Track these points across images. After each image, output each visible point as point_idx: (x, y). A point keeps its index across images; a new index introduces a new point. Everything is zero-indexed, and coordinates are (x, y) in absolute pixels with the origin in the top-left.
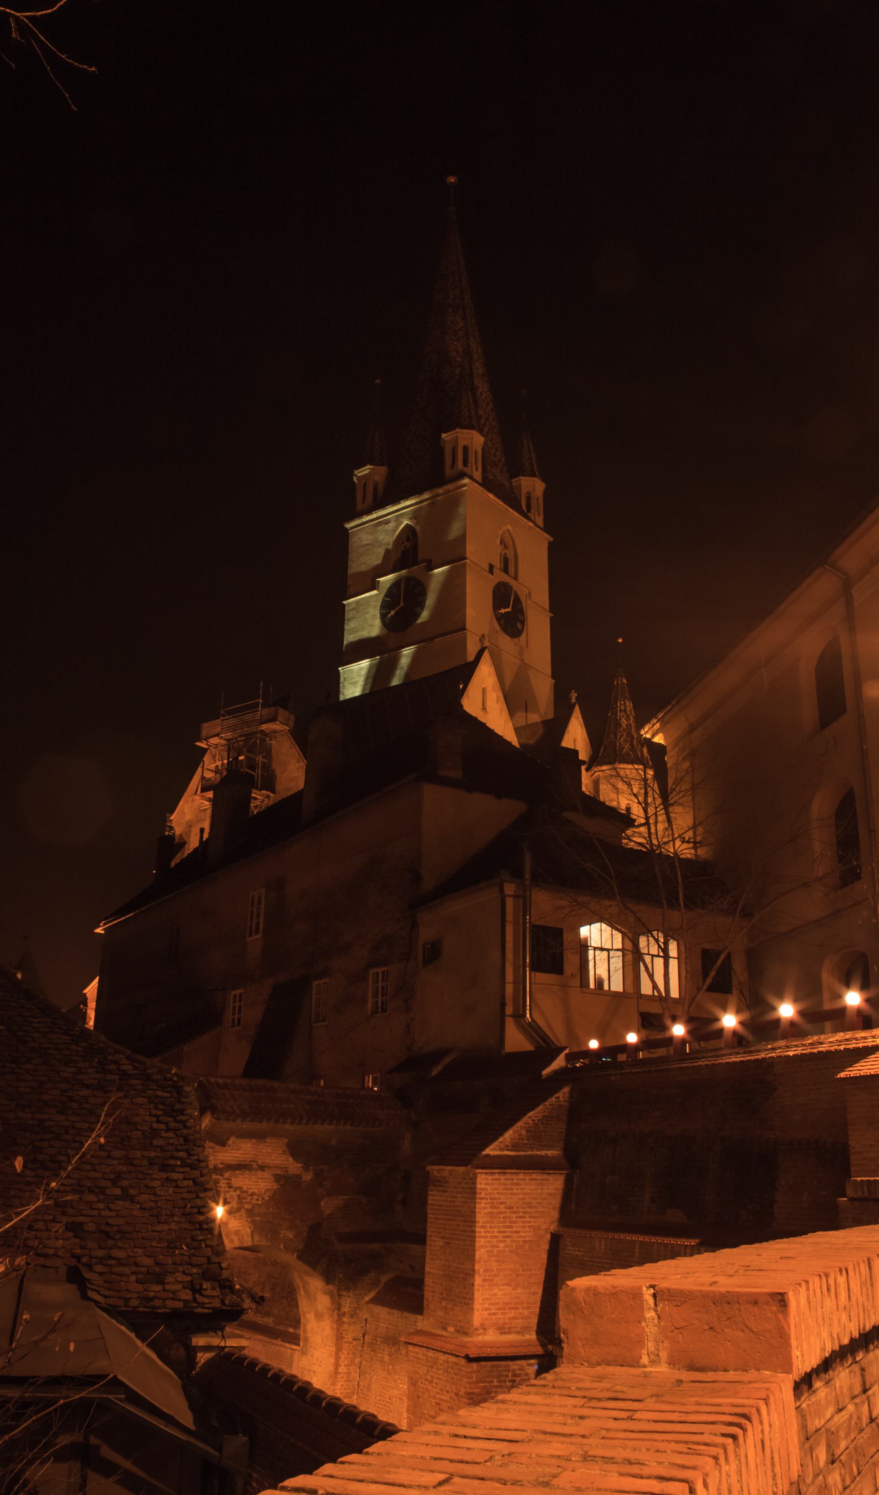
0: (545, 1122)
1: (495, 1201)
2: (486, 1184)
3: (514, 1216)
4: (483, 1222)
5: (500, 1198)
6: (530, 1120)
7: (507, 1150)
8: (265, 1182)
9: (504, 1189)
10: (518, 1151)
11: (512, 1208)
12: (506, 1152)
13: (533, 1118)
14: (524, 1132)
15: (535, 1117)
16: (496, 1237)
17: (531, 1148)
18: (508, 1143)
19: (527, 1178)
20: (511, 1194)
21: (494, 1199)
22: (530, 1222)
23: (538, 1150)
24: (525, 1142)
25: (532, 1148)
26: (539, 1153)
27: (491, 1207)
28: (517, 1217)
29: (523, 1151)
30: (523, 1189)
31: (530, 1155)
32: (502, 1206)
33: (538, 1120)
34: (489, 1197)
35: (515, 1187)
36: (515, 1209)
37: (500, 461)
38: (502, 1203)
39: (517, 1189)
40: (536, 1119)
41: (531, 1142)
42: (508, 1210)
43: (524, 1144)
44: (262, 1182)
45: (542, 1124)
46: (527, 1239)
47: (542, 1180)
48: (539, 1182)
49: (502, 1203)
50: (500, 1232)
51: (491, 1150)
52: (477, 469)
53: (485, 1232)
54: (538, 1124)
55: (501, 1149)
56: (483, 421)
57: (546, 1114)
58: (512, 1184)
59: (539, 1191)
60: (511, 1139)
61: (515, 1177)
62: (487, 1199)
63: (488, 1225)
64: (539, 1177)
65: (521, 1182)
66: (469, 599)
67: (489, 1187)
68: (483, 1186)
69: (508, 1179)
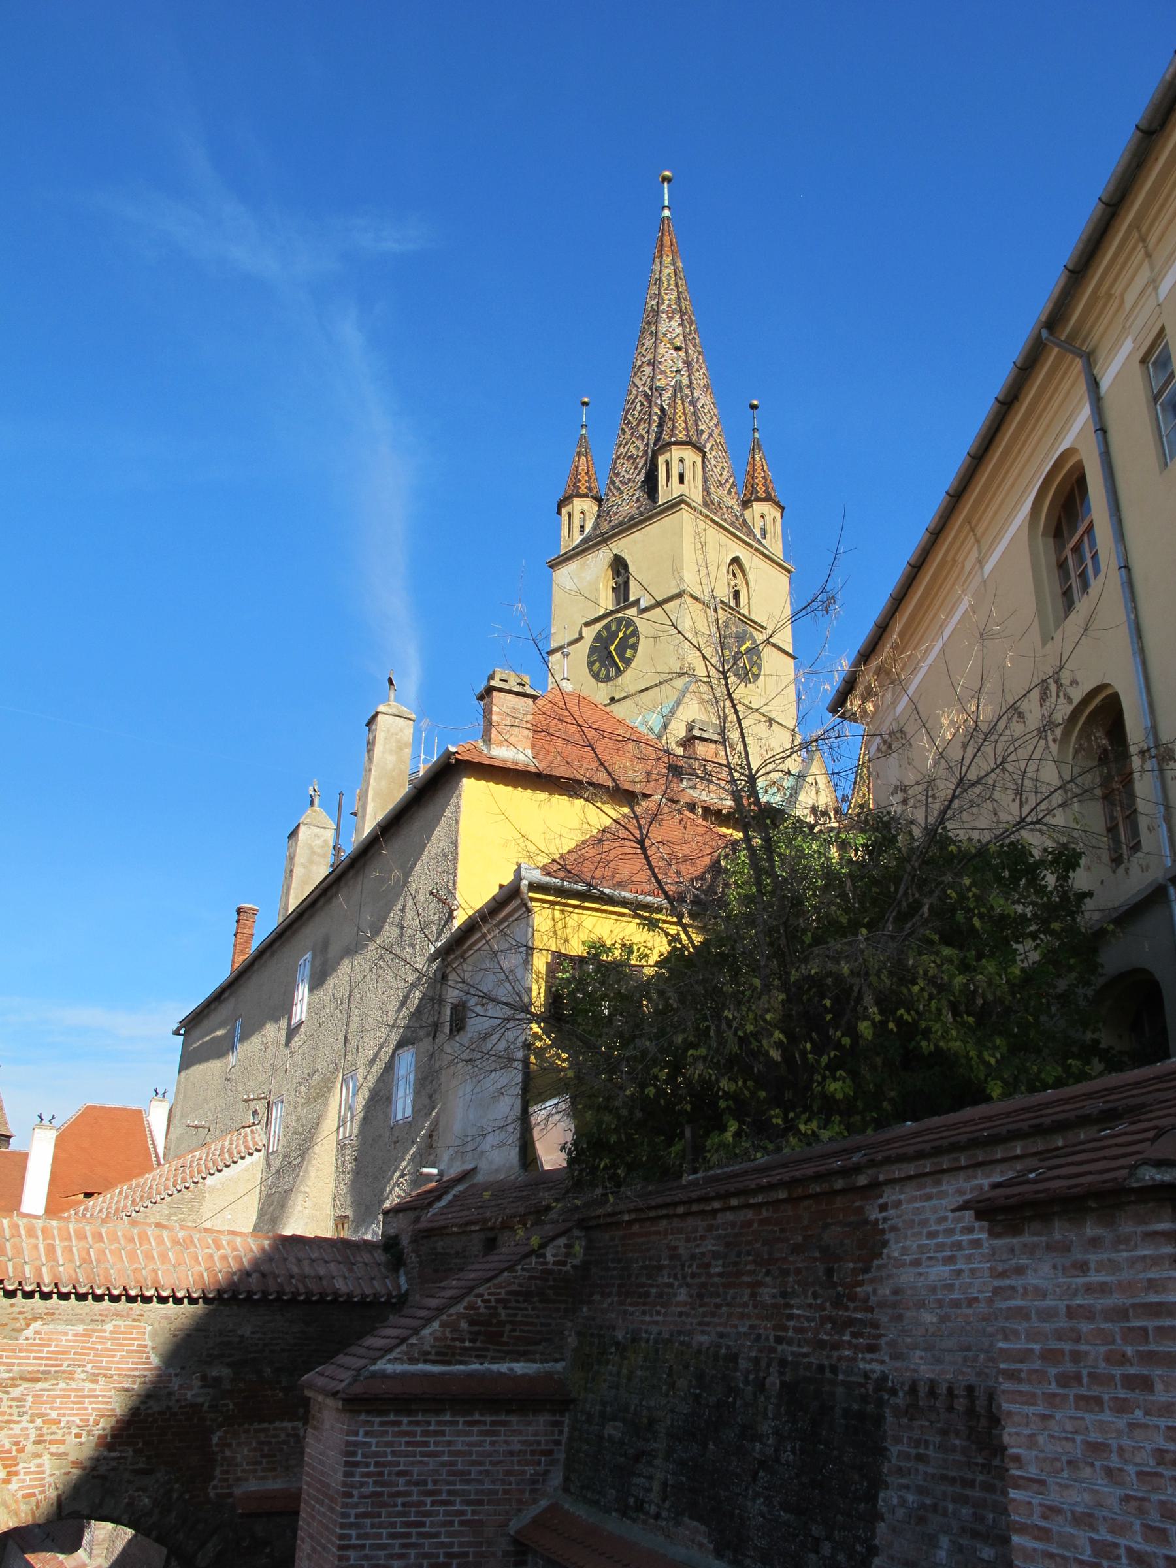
0: (513, 1304)
1: (386, 1470)
2: (367, 1434)
3: (429, 1500)
4: (357, 1516)
5: (398, 1464)
6: (479, 1300)
7: (426, 1361)
8: (96, 1403)
9: (408, 1443)
10: (449, 1363)
11: (425, 1483)
12: (421, 1367)
13: (486, 1297)
14: (464, 1325)
15: (489, 1294)
16: (383, 1547)
17: (477, 1357)
18: (427, 1348)
19: (461, 1420)
20: (423, 1454)
21: (384, 1465)
22: (463, 1513)
23: (494, 1360)
24: (467, 1344)
25: (481, 1358)
26: (494, 1367)
27: (376, 1483)
28: (433, 1503)
29: (461, 1363)
30: (449, 1443)
31: (470, 1375)
32: (401, 1480)
33: (498, 1301)
34: (372, 1461)
35: (432, 1440)
36: (430, 1487)
37: (727, 481)
38: (400, 1474)
39: (436, 1444)
40: (492, 1298)
41: (478, 1344)
42: (415, 1489)
43: (466, 1349)
44: (91, 1403)
45: (505, 1308)
46: (456, 1549)
47: (493, 1423)
48: (488, 1428)
49: (400, 1474)
50: (392, 1536)
51: (389, 1361)
52: (696, 487)
53: (359, 1537)
54: (496, 1308)
55: (412, 1360)
56: (705, 436)
57: (515, 1288)
58: (426, 1433)
59: (488, 1447)
60: (436, 1339)
61: (433, 1419)
62: (367, 1465)
63: (368, 1521)
64: (488, 1419)
65: (447, 1429)
67: (374, 1440)
68: (360, 1438)
69: (418, 1423)
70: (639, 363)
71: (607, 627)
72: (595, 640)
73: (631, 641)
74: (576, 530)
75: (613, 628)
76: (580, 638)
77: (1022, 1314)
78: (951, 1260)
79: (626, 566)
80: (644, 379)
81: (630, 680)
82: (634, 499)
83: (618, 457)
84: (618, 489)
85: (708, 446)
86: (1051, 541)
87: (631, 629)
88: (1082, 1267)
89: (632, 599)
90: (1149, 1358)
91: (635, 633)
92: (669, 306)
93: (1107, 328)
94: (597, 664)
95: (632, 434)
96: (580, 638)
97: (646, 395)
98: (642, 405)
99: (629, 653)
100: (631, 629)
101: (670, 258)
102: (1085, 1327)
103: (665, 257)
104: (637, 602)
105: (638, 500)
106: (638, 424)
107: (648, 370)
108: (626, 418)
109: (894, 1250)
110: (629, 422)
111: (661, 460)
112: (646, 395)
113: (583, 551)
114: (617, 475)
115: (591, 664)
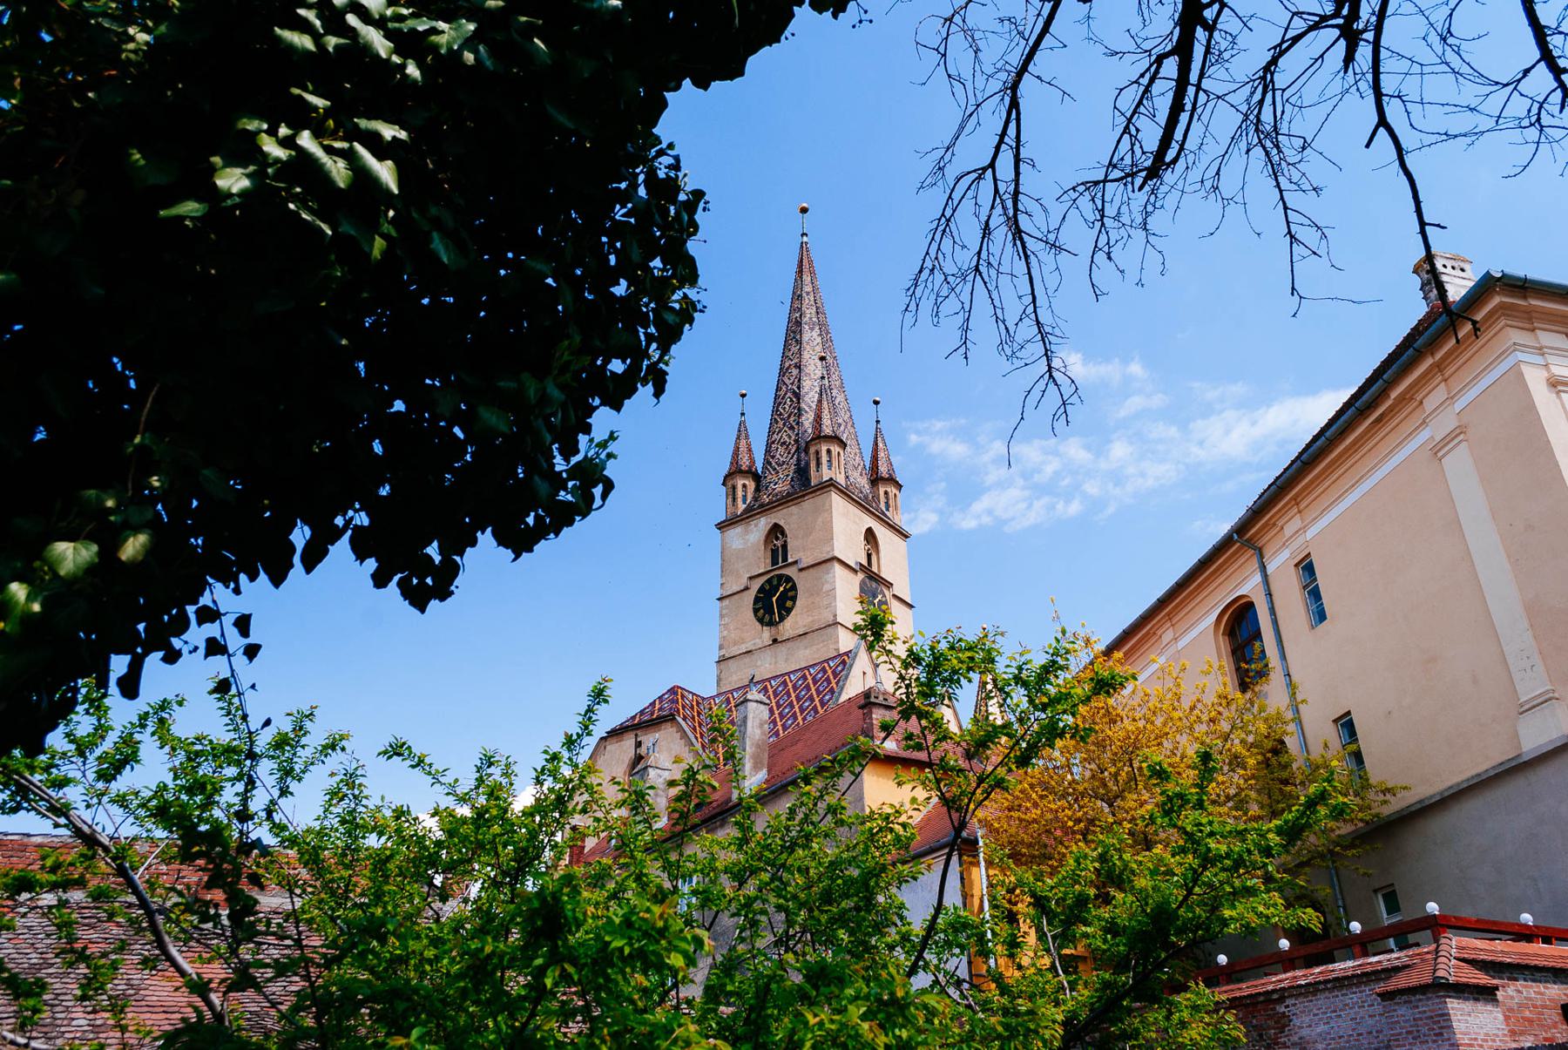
66: (839, 592)
70: (787, 365)
71: (769, 581)
72: (759, 592)
73: (790, 594)
74: (740, 501)
75: (775, 583)
76: (747, 589)
77: (1398, 1022)
78: (1328, 1023)
79: (783, 533)
80: (792, 379)
81: (790, 626)
82: (789, 478)
83: (773, 442)
84: (775, 469)
85: (845, 435)
86: (1227, 638)
87: (790, 585)
88: (1417, 1007)
89: (790, 560)
90: (1441, 1028)
91: (794, 588)
92: (811, 318)
93: (1272, 537)
94: (762, 611)
95: (784, 425)
96: (747, 589)
97: (794, 393)
98: (791, 400)
99: (789, 604)
100: (790, 585)
101: (809, 279)
102: (1420, 1023)
103: (804, 277)
104: (796, 562)
105: (792, 480)
106: (789, 416)
107: (795, 372)
108: (778, 410)
109: (1296, 1022)
110: (781, 414)
111: (812, 450)
112: (794, 393)
113: (747, 518)
114: (773, 457)
115: (756, 611)
